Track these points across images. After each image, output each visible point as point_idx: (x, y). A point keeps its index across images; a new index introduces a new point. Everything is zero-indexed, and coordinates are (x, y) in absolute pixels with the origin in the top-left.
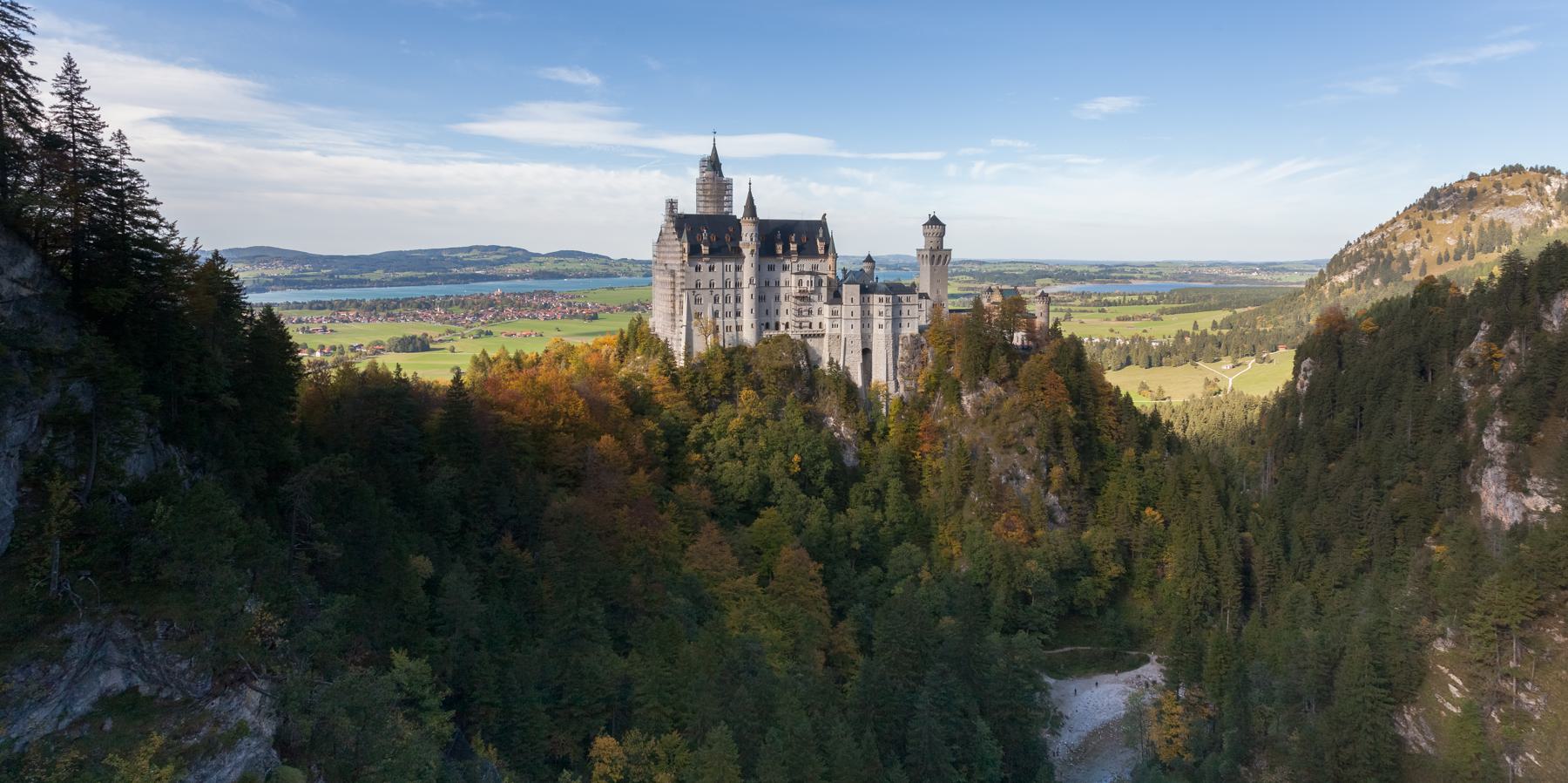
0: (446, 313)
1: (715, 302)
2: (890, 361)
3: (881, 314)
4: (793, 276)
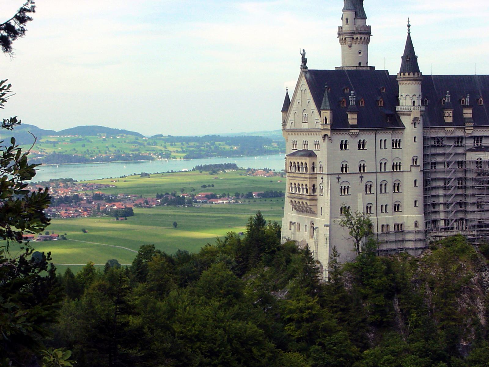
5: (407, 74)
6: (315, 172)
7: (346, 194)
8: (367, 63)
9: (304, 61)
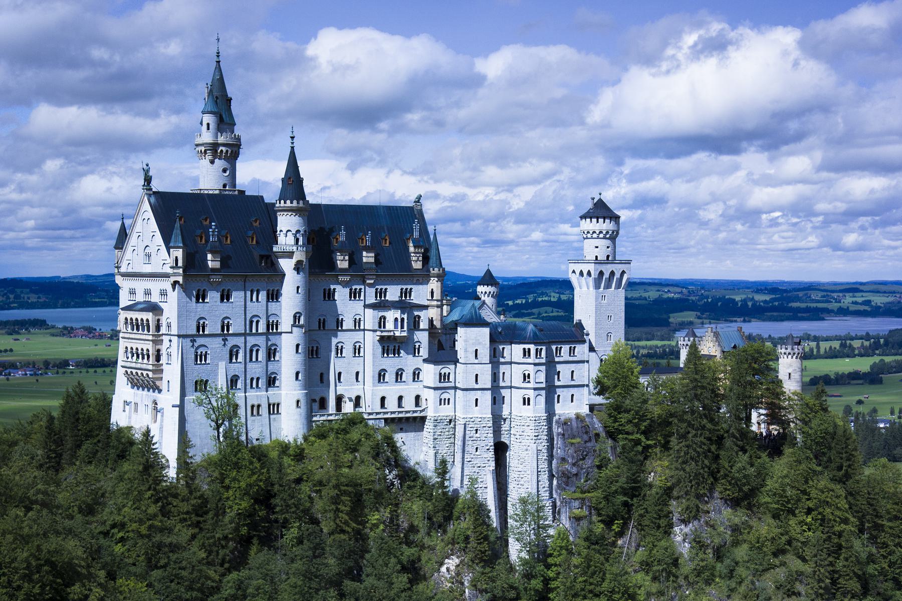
1: (231, 362)
2: (544, 466)
3: (526, 377)
4: (369, 312)
5: (288, 202)
6: (161, 333)
7: (203, 362)
8: (234, 185)
9: (148, 180)
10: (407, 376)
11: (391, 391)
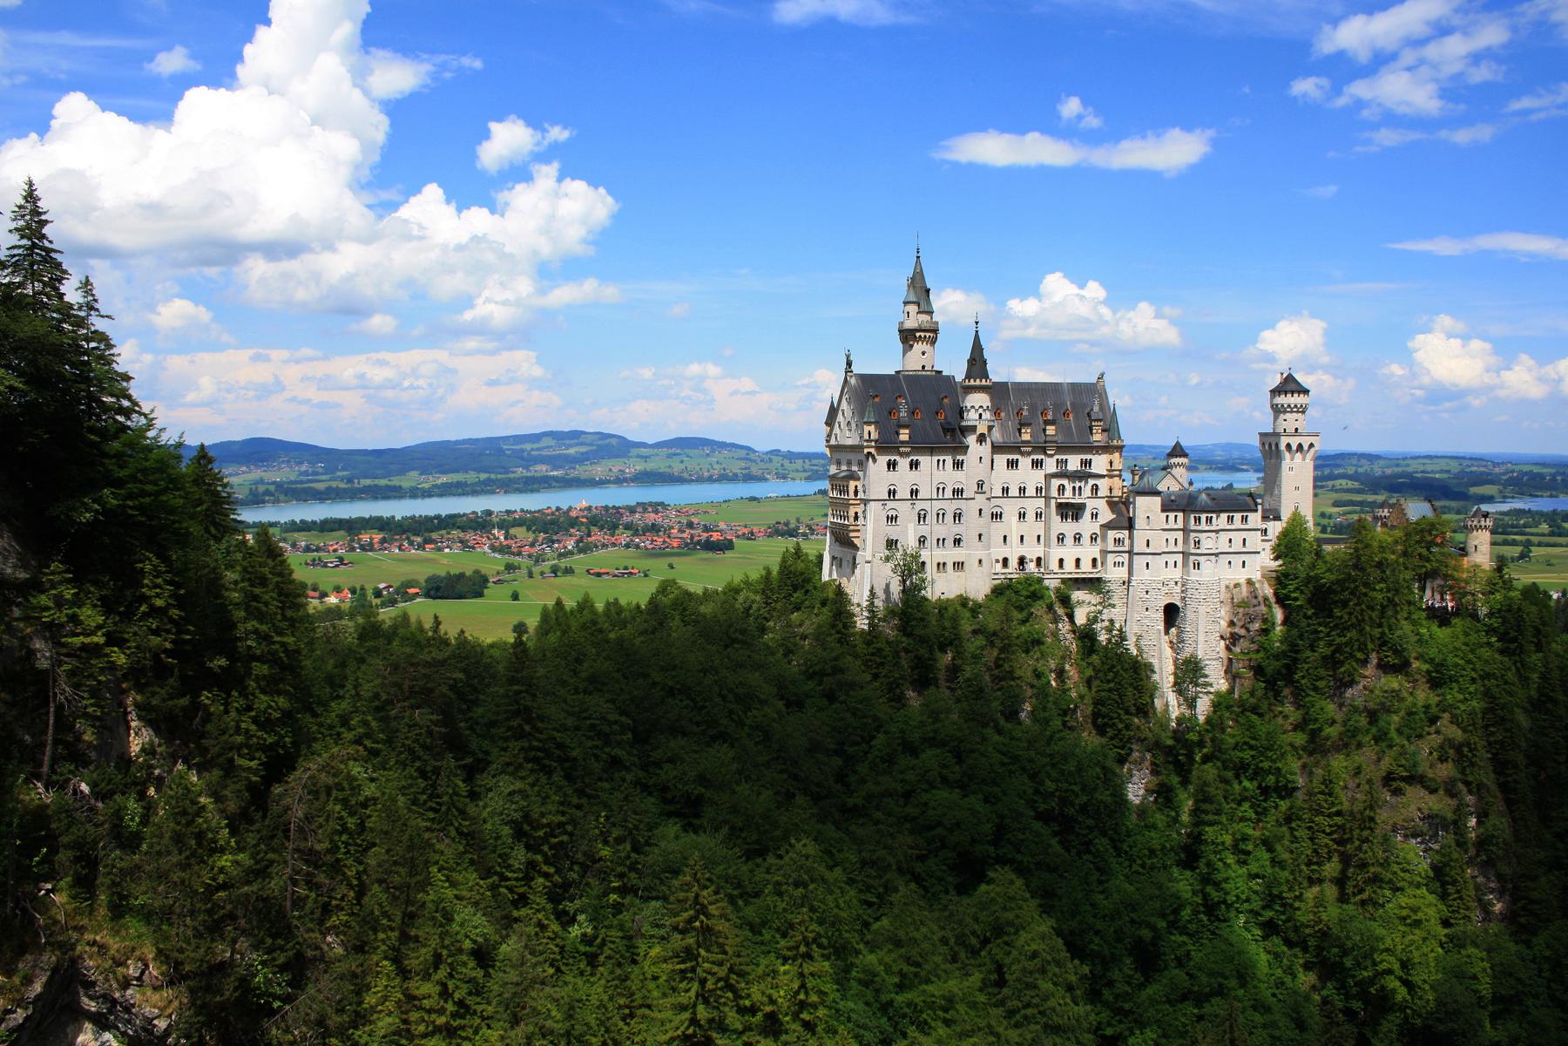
0: (506, 538)
9: (849, 364)
10: (1086, 539)
11: (1069, 552)
